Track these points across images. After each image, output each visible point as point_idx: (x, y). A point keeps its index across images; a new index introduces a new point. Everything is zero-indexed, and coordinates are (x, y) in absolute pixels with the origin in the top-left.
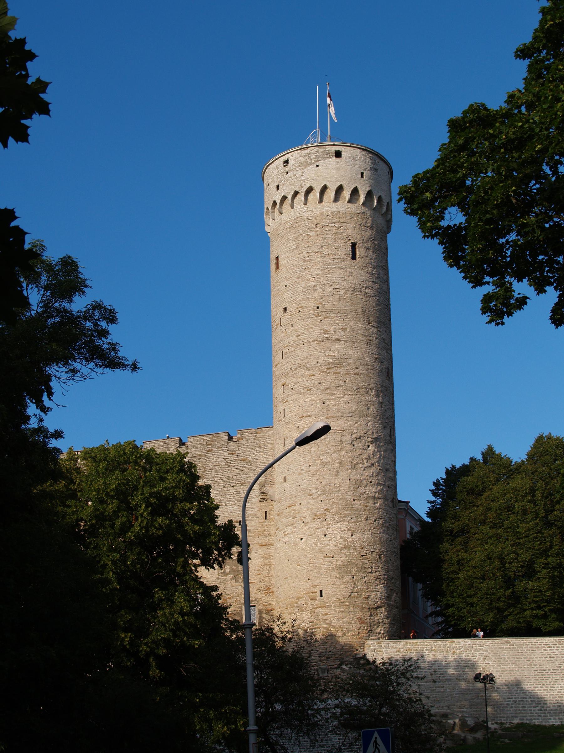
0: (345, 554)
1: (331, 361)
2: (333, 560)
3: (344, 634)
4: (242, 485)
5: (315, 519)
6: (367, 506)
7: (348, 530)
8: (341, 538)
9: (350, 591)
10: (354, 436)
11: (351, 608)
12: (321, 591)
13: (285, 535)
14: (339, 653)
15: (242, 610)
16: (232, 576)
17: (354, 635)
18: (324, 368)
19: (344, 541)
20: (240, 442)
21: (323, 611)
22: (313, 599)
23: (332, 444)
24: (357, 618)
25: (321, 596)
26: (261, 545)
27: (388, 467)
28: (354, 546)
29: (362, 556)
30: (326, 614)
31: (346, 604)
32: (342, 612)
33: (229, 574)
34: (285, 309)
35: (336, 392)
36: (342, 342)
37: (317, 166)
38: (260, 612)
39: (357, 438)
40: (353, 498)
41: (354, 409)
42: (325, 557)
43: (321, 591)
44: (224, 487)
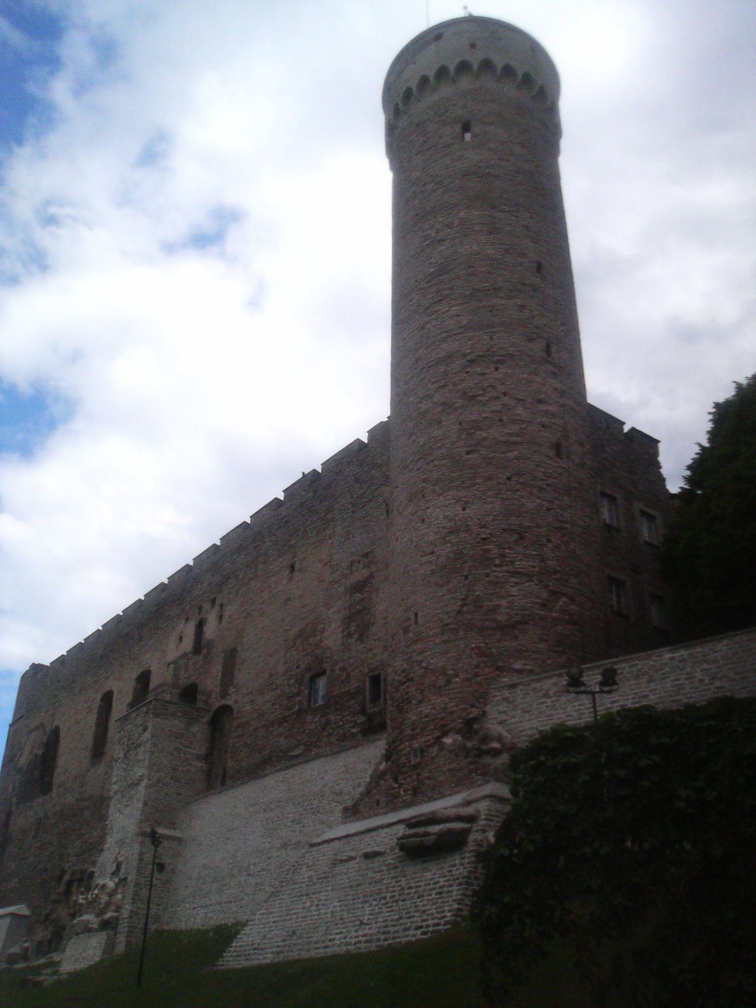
0: (451, 543)
1: (432, 270)
2: (433, 558)
3: (449, 682)
4: (371, 501)
5: (410, 500)
6: (493, 458)
7: (457, 502)
8: (445, 517)
9: (460, 603)
10: (468, 358)
11: (461, 633)
12: (416, 614)
14: (439, 716)
15: (365, 685)
16: (356, 636)
17: (467, 679)
18: (423, 285)
19: (451, 521)
21: (419, 647)
22: (406, 630)
24: (472, 649)
27: (542, 396)
28: (467, 526)
29: (483, 539)
30: (422, 652)
31: (451, 626)
32: (445, 642)
33: (354, 633)
35: (438, 308)
39: (472, 361)
40: (466, 449)
41: (465, 322)
42: (422, 557)
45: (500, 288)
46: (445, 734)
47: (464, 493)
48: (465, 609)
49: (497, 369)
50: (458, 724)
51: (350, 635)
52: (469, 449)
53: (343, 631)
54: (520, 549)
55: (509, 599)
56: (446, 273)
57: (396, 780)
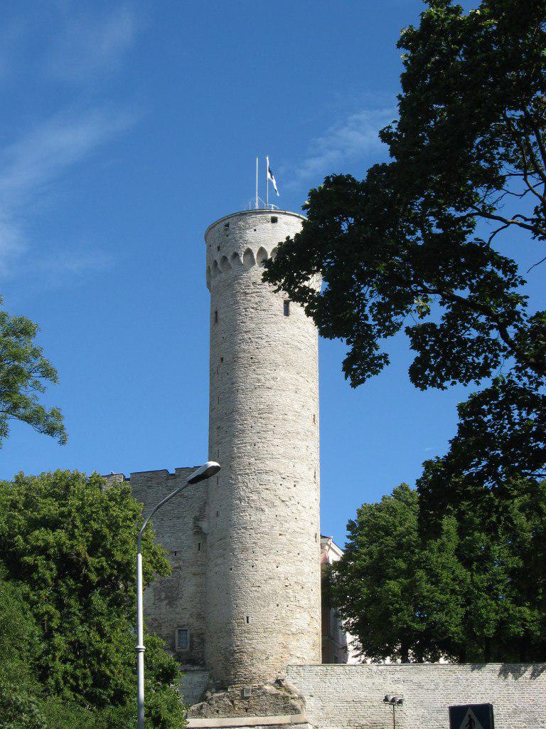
3: (267, 658)
4: (178, 519)
12: (247, 617)
13: (216, 566)
20: (178, 480)
23: (261, 483)
25: (248, 622)
26: (194, 574)
34: (222, 359)
36: (273, 391)
37: (255, 230)
38: (192, 636)
43: (247, 617)
44: (162, 520)
45: (298, 433)
46: (266, 684)
47: (278, 558)
48: (276, 621)
49: (295, 486)
50: (272, 680)
51: (160, 600)
52: (280, 533)
53: (155, 596)
54: (301, 593)
55: (296, 620)
56: (272, 413)
57: (232, 702)
